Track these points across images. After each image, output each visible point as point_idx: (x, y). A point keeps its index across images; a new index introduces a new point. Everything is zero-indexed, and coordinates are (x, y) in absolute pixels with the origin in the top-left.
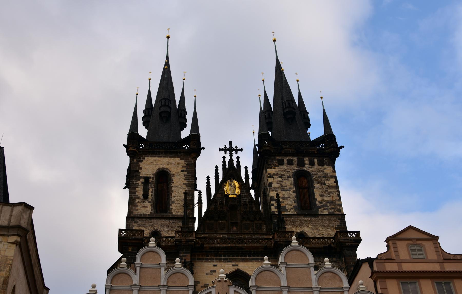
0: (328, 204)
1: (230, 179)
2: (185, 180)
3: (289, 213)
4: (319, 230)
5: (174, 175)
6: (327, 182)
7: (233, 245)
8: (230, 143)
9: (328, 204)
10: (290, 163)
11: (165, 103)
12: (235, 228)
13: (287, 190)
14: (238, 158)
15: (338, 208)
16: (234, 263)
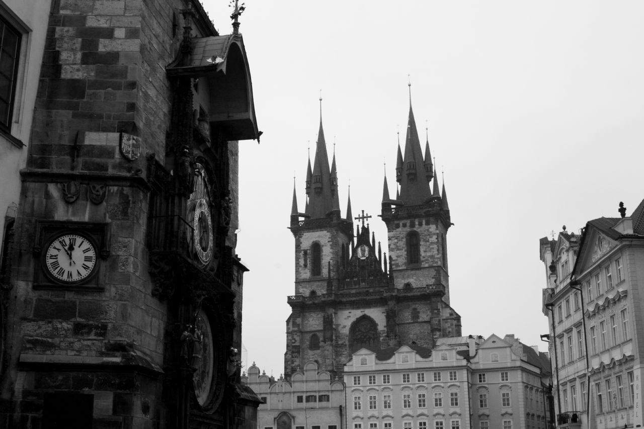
0: (429, 259)
1: (361, 244)
2: (331, 249)
3: (400, 268)
4: (420, 280)
5: (323, 245)
6: (430, 239)
7: (360, 298)
8: (363, 211)
9: (429, 259)
10: (405, 225)
11: (317, 179)
12: (364, 284)
13: (400, 250)
14: (368, 224)
15: (436, 260)
16: (362, 310)
